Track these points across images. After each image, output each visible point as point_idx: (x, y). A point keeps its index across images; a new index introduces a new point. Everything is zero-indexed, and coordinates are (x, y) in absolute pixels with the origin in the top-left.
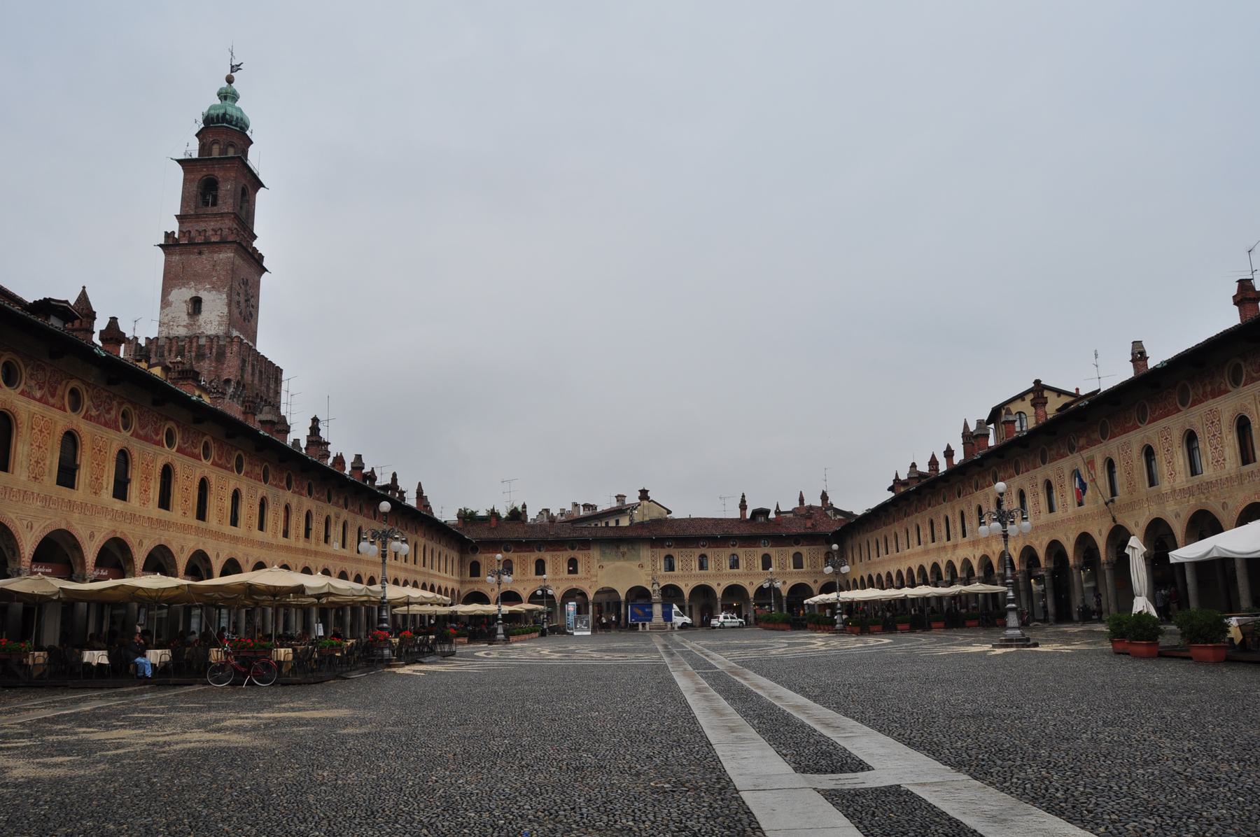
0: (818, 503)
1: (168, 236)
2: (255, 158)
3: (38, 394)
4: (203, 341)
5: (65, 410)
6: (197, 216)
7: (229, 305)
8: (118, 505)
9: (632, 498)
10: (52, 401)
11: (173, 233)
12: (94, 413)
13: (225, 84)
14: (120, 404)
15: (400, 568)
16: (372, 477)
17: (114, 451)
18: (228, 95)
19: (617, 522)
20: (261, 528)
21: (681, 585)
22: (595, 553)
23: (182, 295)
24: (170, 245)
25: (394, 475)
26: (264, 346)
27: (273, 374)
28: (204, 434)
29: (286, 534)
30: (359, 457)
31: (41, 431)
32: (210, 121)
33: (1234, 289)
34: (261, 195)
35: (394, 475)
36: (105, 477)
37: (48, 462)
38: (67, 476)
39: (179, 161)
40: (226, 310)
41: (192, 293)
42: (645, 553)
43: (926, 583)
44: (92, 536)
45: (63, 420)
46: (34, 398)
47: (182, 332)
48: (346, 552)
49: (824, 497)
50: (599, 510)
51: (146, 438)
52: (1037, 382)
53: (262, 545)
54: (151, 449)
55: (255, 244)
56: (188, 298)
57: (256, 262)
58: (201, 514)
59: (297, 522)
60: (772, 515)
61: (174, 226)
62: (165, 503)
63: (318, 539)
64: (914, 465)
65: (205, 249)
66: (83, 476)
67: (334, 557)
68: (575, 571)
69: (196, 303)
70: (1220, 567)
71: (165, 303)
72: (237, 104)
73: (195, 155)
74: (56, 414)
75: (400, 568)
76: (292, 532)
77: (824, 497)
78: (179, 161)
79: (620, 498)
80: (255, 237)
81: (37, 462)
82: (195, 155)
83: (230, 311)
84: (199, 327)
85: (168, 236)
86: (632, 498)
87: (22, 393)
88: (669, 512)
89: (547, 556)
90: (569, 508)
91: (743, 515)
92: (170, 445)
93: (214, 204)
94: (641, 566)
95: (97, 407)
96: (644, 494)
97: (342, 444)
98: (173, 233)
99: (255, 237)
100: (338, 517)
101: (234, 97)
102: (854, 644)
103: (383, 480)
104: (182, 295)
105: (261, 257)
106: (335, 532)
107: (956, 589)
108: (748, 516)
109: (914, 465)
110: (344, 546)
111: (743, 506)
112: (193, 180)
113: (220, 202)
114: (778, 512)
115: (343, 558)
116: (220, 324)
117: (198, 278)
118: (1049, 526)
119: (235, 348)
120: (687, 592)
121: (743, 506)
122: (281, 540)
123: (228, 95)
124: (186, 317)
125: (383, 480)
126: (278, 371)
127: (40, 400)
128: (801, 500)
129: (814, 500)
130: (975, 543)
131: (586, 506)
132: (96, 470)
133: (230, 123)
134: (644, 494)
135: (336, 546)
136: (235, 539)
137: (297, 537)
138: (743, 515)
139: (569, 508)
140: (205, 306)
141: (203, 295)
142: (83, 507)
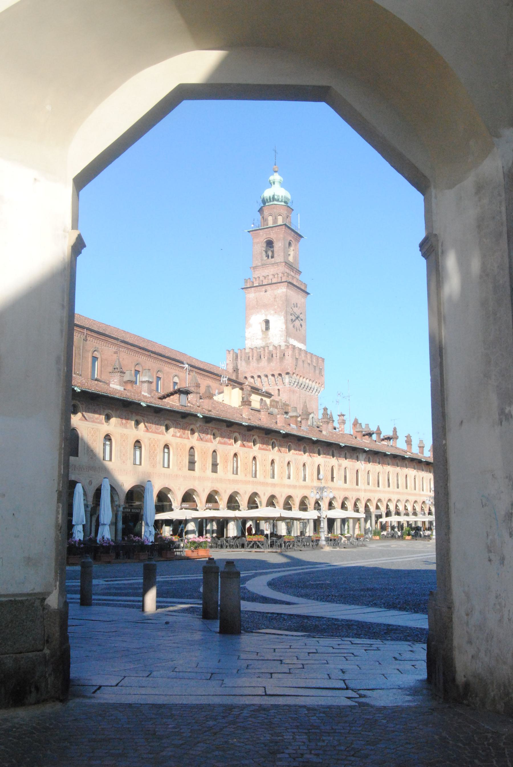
4: (271, 348)
5: (189, 439)
6: (263, 265)
10: (184, 436)
14: (212, 431)
15: (393, 492)
25: (395, 430)
28: (253, 436)
31: (181, 449)
35: (395, 430)
36: (208, 464)
37: (184, 462)
40: (284, 327)
41: (264, 318)
44: (204, 490)
46: (177, 437)
53: (289, 486)
63: (326, 481)
65: (268, 287)
67: (339, 489)
75: (393, 492)
81: (180, 462)
83: (287, 328)
84: (269, 338)
93: (272, 257)
100: (340, 466)
104: (256, 320)
112: (258, 243)
113: (275, 255)
115: (345, 490)
117: (265, 306)
119: (290, 352)
122: (303, 483)
124: (260, 333)
127: (179, 437)
132: (203, 462)
133: (278, 200)
136: (274, 485)
137: (312, 480)
140: (271, 325)
142: (200, 478)
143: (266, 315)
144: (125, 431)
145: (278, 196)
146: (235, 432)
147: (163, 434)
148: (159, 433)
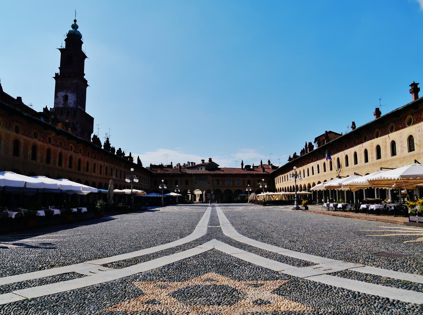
0: (267, 164)
1: (57, 74)
2: (84, 48)
3: (42, 140)
7: (77, 98)
8: (60, 168)
9: (207, 161)
10: (45, 141)
11: (58, 73)
12: (54, 143)
13: (74, 23)
16: (124, 154)
17: (58, 153)
18: (75, 26)
19: (201, 169)
20: (94, 172)
21: (221, 189)
22: (194, 178)
23: (62, 94)
24: (57, 77)
25: (130, 153)
26: (89, 110)
27: (91, 120)
29: (100, 174)
30: (120, 149)
32: (68, 35)
33: (374, 110)
34: (86, 60)
35: (130, 153)
38: (48, 161)
39: (59, 49)
40: (76, 99)
41: (65, 93)
42: (210, 178)
43: (288, 191)
45: (47, 146)
47: (61, 106)
48: (117, 178)
49: (269, 162)
50: (196, 164)
51: (66, 149)
52: (326, 132)
54: (67, 152)
55: (85, 77)
56: (63, 95)
57: (85, 84)
58: (79, 169)
59: (104, 170)
60: (251, 167)
61: (58, 71)
62: (70, 166)
64: (295, 153)
66: (52, 160)
68: (188, 184)
69: (66, 98)
70: (315, 192)
71: (56, 97)
72: (78, 30)
73: (64, 46)
74: (45, 145)
76: (102, 173)
77: (269, 162)
78: (59, 49)
79: (203, 161)
80: (85, 75)
82: (64, 46)
85: (57, 74)
86: (207, 161)
87: (39, 140)
88: (219, 166)
89: (179, 179)
90: (186, 163)
91: (242, 167)
92: (71, 150)
94: (209, 183)
95: (54, 141)
96: (210, 160)
97: (115, 145)
98: (58, 73)
99: (85, 75)
100: (115, 168)
101: (77, 27)
102: (262, 207)
103: (127, 155)
105: (87, 81)
106: (114, 173)
107: (291, 193)
108: (244, 167)
109: (295, 153)
110: (116, 176)
111: (242, 164)
114: (253, 167)
116: (74, 104)
118: (324, 176)
120: (223, 191)
121: (242, 164)
123: (75, 26)
124: (62, 101)
125: (127, 155)
126: (93, 119)
127: (43, 141)
128: (261, 162)
129: (265, 162)
130: (307, 179)
131: (192, 163)
134: (210, 160)
135: (114, 177)
138: (242, 167)
139: (186, 163)
140: (69, 98)
141: (69, 94)
143: (66, 93)
144: (9, 132)
145: (76, 34)
146: (71, 143)
147: (32, 138)
148: (30, 137)
